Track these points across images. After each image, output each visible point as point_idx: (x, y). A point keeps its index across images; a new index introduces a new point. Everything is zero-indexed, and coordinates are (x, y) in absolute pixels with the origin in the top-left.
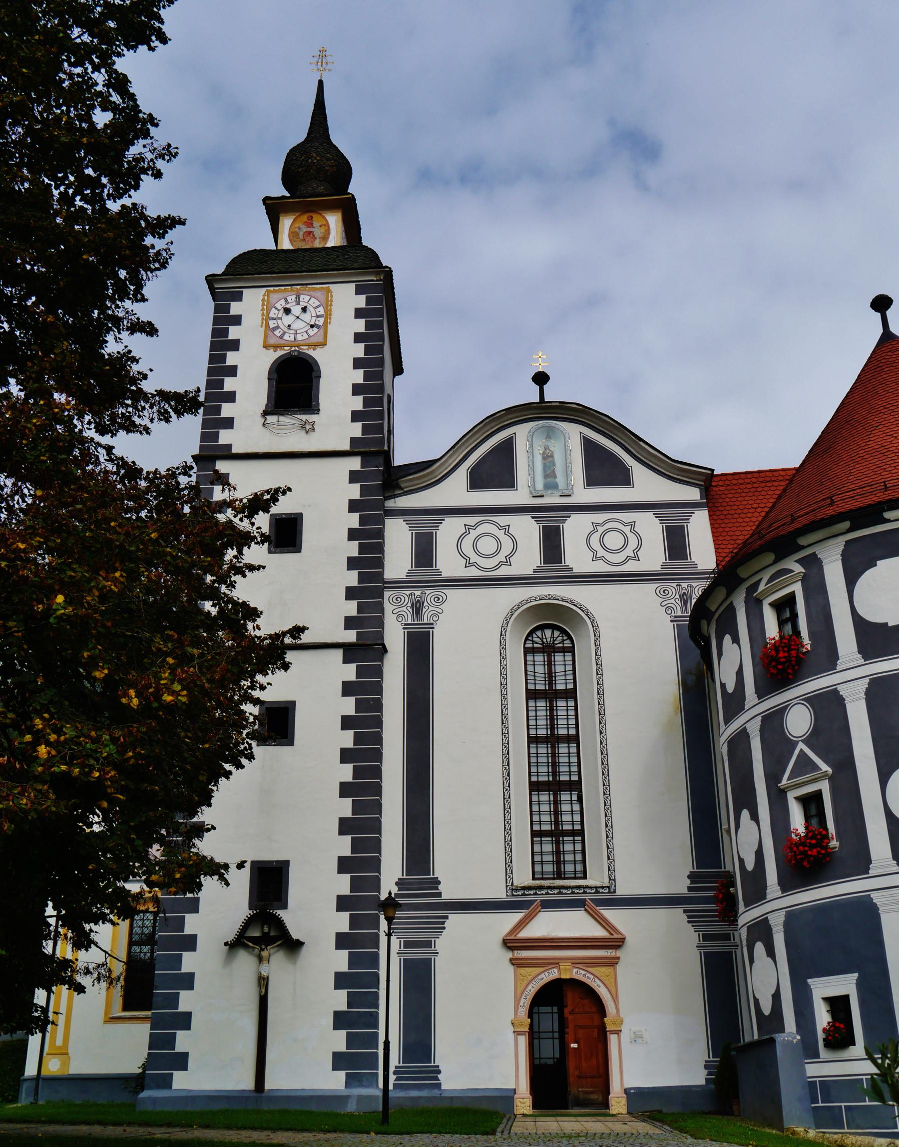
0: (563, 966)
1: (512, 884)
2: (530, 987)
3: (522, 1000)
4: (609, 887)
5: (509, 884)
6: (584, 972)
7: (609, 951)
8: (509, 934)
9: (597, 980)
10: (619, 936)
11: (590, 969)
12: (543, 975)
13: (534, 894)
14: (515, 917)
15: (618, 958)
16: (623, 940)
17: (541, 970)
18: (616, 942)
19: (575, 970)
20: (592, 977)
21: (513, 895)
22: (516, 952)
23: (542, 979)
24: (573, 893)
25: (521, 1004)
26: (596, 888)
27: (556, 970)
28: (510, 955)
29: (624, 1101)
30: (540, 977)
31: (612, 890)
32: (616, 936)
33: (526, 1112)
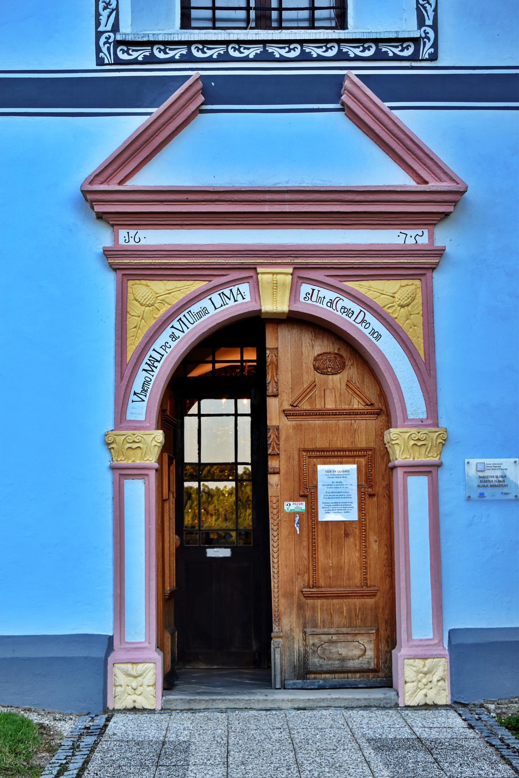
0: (266, 275)
1: (115, 28)
2: (164, 337)
3: (141, 377)
4: (416, 41)
5: (106, 26)
6: (330, 295)
7: (412, 233)
8: (98, 176)
9: (369, 317)
10: (446, 185)
11: (352, 285)
12: (205, 303)
13: (183, 60)
14: (125, 126)
15: (440, 253)
16: (456, 196)
17: (196, 286)
18: (436, 205)
19: (306, 288)
20: (356, 308)
21: (118, 61)
22: (123, 233)
23: (205, 311)
24: (305, 57)
25: (137, 387)
26: (377, 41)
27: (245, 288)
28: (104, 238)
29: (441, 667)
30: (195, 308)
31: (426, 51)
32: (434, 185)
33: (142, 702)
